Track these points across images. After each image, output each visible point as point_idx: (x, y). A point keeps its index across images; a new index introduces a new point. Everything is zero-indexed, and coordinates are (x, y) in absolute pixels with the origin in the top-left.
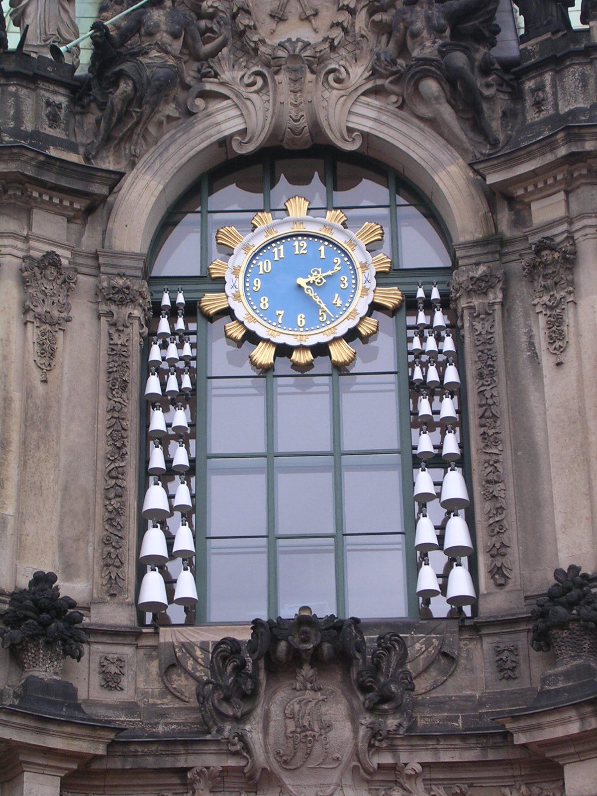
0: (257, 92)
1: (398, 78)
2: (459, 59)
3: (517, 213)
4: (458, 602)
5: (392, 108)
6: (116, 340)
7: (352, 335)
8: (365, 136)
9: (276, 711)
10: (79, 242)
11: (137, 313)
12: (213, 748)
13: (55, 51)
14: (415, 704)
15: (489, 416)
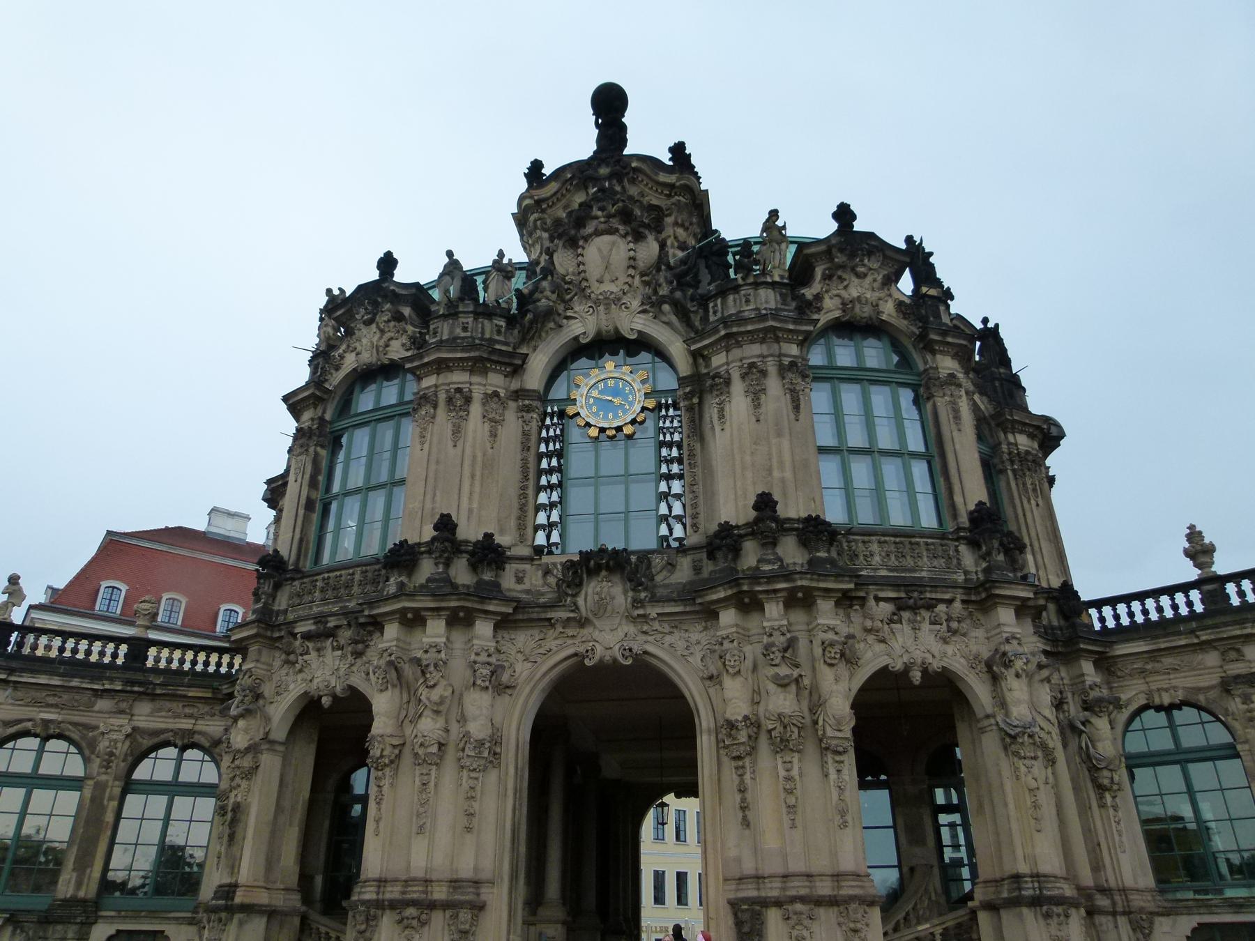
0: (590, 315)
1: (653, 305)
2: (678, 294)
3: (706, 362)
4: (679, 540)
5: (651, 318)
6: (527, 428)
7: (633, 422)
8: (639, 332)
9: (590, 590)
10: (509, 387)
11: (535, 416)
12: (563, 609)
13: (497, 301)
14: (655, 586)
15: (692, 455)
